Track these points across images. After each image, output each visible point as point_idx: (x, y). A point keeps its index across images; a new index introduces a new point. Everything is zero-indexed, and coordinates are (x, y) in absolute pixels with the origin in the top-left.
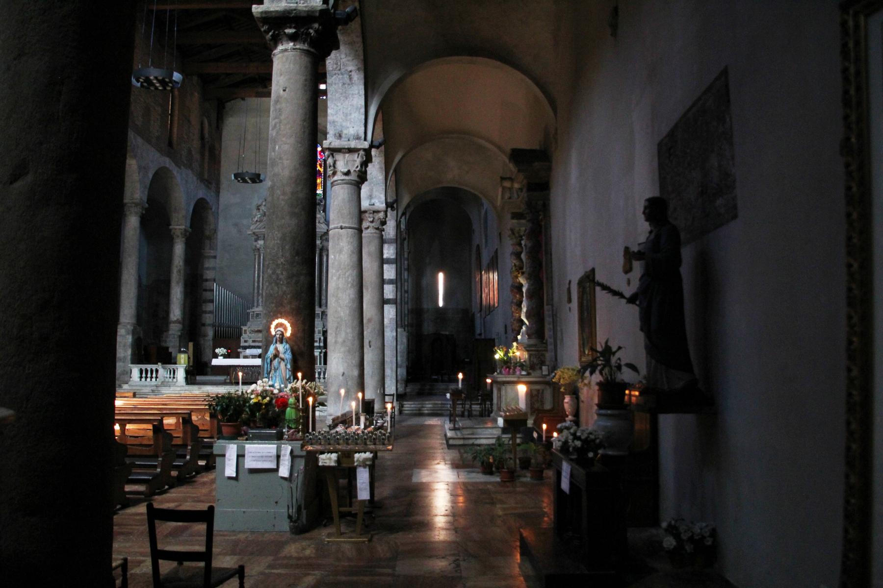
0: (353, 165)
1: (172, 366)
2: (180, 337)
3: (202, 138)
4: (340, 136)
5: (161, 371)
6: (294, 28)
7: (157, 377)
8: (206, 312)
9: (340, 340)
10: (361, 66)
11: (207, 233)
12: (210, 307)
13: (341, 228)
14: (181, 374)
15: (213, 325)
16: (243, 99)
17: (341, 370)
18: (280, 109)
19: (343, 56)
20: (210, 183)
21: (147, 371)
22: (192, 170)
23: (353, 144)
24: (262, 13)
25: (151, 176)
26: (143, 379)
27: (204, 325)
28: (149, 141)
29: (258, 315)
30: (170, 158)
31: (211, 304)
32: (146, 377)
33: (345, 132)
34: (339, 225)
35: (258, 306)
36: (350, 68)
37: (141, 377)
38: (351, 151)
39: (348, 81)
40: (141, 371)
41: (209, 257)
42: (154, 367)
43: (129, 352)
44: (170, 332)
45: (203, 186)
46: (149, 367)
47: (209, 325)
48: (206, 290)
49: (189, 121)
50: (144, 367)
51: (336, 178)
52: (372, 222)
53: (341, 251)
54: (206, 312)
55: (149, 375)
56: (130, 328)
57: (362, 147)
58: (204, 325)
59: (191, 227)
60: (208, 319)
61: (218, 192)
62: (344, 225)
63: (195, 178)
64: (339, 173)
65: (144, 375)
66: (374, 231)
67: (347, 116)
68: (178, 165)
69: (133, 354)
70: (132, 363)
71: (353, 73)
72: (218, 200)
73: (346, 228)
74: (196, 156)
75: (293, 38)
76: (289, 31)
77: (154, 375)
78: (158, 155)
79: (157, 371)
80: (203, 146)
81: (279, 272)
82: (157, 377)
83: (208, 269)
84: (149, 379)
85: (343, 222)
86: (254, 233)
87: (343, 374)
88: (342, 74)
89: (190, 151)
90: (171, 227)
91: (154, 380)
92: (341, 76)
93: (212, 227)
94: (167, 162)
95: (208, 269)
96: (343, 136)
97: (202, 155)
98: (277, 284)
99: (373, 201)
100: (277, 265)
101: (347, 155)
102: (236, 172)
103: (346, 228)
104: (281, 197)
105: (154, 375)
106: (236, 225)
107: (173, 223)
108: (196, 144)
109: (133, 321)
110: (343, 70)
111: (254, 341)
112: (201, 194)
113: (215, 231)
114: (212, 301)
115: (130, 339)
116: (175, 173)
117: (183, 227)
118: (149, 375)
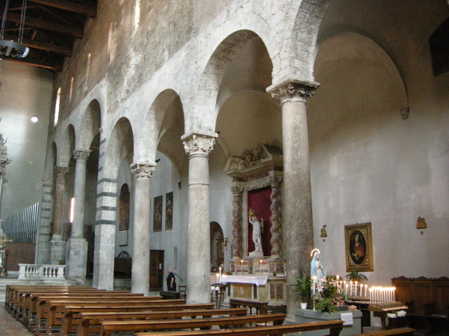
0: (207, 146)
4: (200, 127)
6: (304, 91)
9: (202, 254)
10: (218, 88)
13: (203, 185)
17: (203, 274)
18: (299, 133)
19: (211, 80)
23: (209, 133)
24: (294, 80)
33: (203, 125)
34: (202, 182)
36: (211, 88)
38: (208, 137)
39: (208, 95)
51: (197, 152)
52: (147, 173)
53: (202, 199)
57: (215, 136)
62: (204, 183)
64: (200, 150)
66: (147, 179)
67: (204, 115)
71: (212, 91)
73: (205, 184)
75: (302, 95)
76: (303, 92)
81: (305, 221)
85: (204, 181)
87: (204, 276)
88: (206, 90)
92: (205, 91)
96: (202, 127)
98: (305, 228)
99: (148, 159)
100: (305, 218)
101: (205, 139)
103: (205, 184)
104: (304, 181)
110: (207, 88)
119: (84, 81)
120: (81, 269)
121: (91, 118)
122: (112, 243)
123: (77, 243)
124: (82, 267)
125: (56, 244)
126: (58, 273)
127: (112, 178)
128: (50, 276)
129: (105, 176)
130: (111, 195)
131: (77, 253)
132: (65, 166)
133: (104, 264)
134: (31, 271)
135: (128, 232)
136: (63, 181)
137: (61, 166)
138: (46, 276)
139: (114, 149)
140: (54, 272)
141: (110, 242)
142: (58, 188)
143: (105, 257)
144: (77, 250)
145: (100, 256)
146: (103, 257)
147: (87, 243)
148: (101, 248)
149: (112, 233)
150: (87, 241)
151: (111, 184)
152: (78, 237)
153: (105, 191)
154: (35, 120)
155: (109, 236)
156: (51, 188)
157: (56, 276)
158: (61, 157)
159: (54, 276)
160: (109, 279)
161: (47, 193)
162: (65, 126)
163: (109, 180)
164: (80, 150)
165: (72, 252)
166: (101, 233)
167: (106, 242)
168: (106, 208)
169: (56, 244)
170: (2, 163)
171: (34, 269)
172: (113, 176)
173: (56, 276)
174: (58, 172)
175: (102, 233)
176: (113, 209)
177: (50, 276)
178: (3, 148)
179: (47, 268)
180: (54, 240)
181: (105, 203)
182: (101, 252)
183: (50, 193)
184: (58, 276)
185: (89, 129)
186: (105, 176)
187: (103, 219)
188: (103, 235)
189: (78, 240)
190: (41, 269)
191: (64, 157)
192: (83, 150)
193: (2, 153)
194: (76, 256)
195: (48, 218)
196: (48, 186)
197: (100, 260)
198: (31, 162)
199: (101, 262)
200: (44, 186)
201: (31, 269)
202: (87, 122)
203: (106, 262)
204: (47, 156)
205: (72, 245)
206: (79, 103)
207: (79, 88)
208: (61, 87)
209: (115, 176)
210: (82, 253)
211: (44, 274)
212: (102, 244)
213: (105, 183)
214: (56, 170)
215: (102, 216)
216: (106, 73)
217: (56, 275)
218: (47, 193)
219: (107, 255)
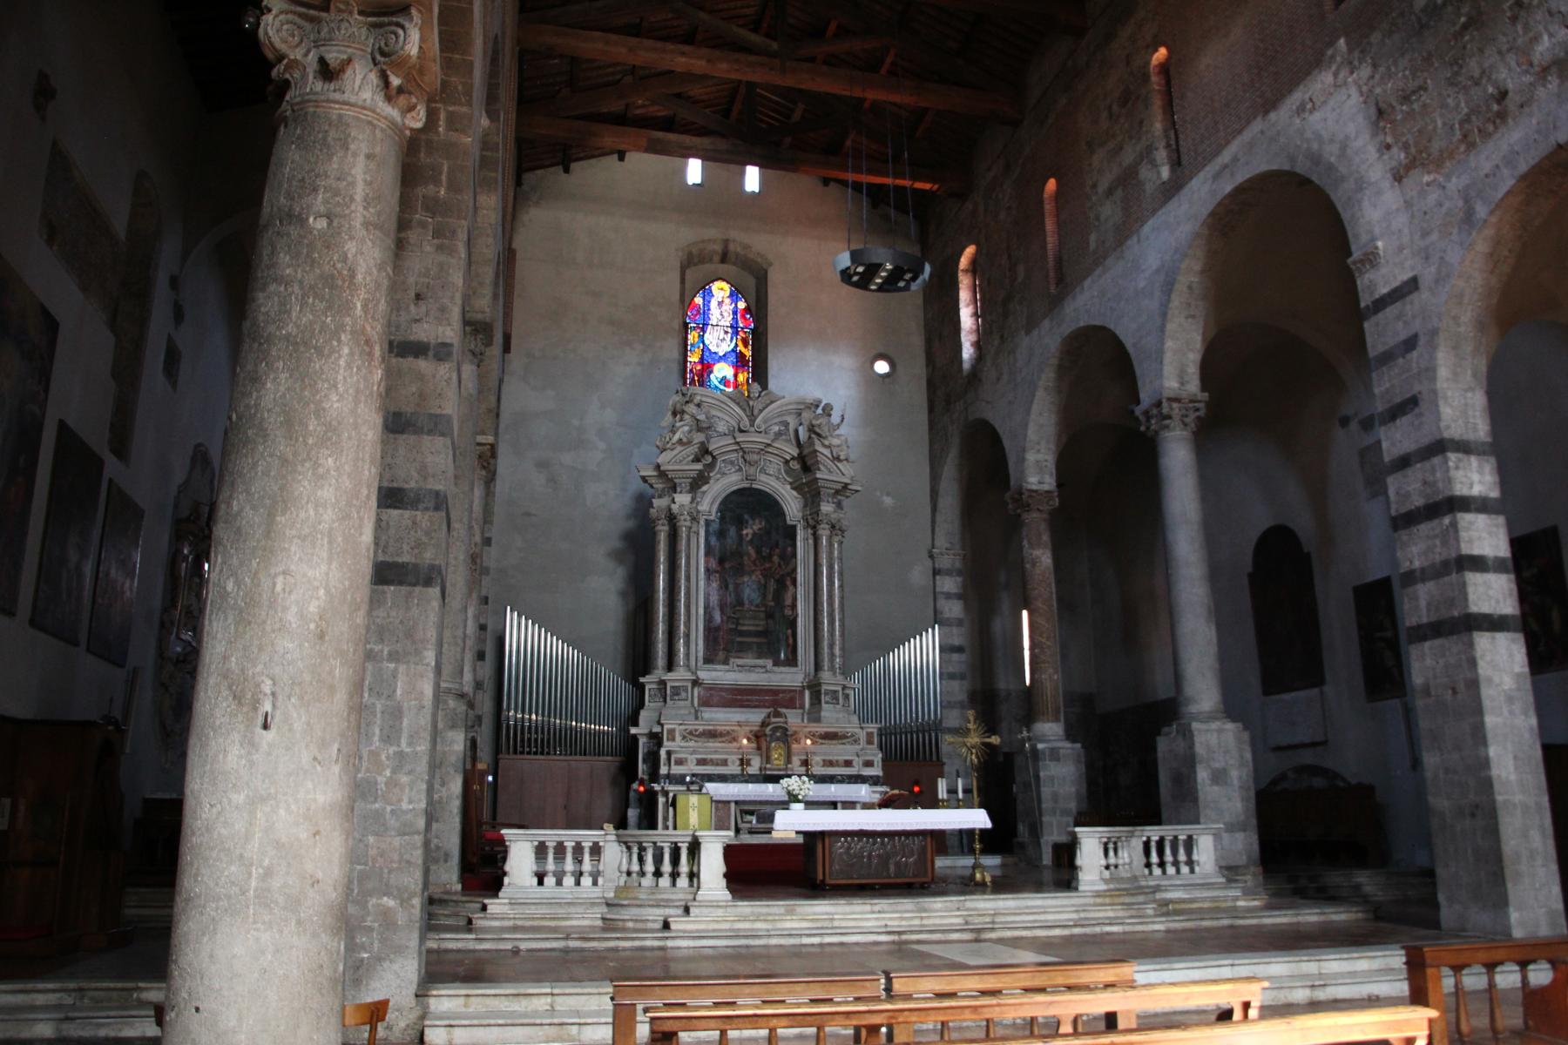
5: (614, 854)
7: (595, 877)
29: (676, 691)
35: (670, 667)
40: (541, 850)
42: (587, 836)
46: (569, 837)
50: (551, 836)
79: (596, 850)
91: (586, 881)
105: (587, 866)
106: (542, 465)
111: (701, 762)
119: (1150, 149)
120: (1240, 836)
121: (1203, 272)
122: (1525, 714)
123: (1213, 739)
124: (1243, 828)
125: (1055, 755)
126: (1195, 857)
127: (1470, 436)
128: (1171, 870)
129: (1448, 427)
130: (1481, 505)
131: (1219, 777)
132: (1046, 487)
133: (1515, 805)
134: (1111, 853)
135: (1322, 693)
136: (1046, 538)
137: (1034, 487)
138: (1157, 871)
139: (1469, 314)
140: (1182, 857)
141: (1517, 707)
142: (1034, 564)
143: (1513, 777)
144: (1217, 765)
145: (1495, 772)
146: (1504, 775)
147: (1246, 736)
148: (1490, 735)
149: (1517, 669)
150: (1246, 728)
151: (1474, 460)
152: (1210, 717)
153: (1460, 490)
154: (882, 367)
155: (1508, 683)
156: (959, 579)
157: (1192, 871)
158: (1031, 457)
159: (1185, 869)
160: (1541, 872)
161: (948, 596)
162: (1044, 343)
163: (1464, 447)
164: (1171, 395)
165: (1202, 775)
166: (1480, 671)
167: (1505, 711)
168: (1478, 564)
169: (1055, 755)
170: (837, 492)
171: (1111, 846)
172: (1475, 429)
173: (1192, 871)
174: (1027, 507)
175: (1483, 669)
176: (1499, 566)
177: (1171, 870)
178: (835, 442)
179: (1155, 838)
180: (1042, 741)
181: (1470, 541)
182: (1492, 751)
183: (959, 597)
184: (1197, 869)
185: (1193, 317)
186: (1448, 427)
187: (1474, 609)
188: (1490, 680)
189: (1215, 725)
190: (1137, 844)
191: (1040, 457)
192: (1184, 395)
193: (838, 459)
194: (1216, 788)
195: (962, 677)
196: (949, 573)
197: (1497, 787)
198: (888, 501)
199: (1499, 798)
200: (936, 572)
201: (1111, 846)
202: (1190, 287)
203: (1518, 798)
204: (935, 478)
205: (1199, 749)
206: (1126, 230)
207: (1110, 192)
208: (978, 245)
209: (1480, 429)
210: (1234, 774)
211: (1148, 865)
212: (1490, 720)
213: (1453, 457)
215: (1472, 597)
216: (1338, 38)
217: (1190, 863)
218: (948, 596)
219: (1516, 768)
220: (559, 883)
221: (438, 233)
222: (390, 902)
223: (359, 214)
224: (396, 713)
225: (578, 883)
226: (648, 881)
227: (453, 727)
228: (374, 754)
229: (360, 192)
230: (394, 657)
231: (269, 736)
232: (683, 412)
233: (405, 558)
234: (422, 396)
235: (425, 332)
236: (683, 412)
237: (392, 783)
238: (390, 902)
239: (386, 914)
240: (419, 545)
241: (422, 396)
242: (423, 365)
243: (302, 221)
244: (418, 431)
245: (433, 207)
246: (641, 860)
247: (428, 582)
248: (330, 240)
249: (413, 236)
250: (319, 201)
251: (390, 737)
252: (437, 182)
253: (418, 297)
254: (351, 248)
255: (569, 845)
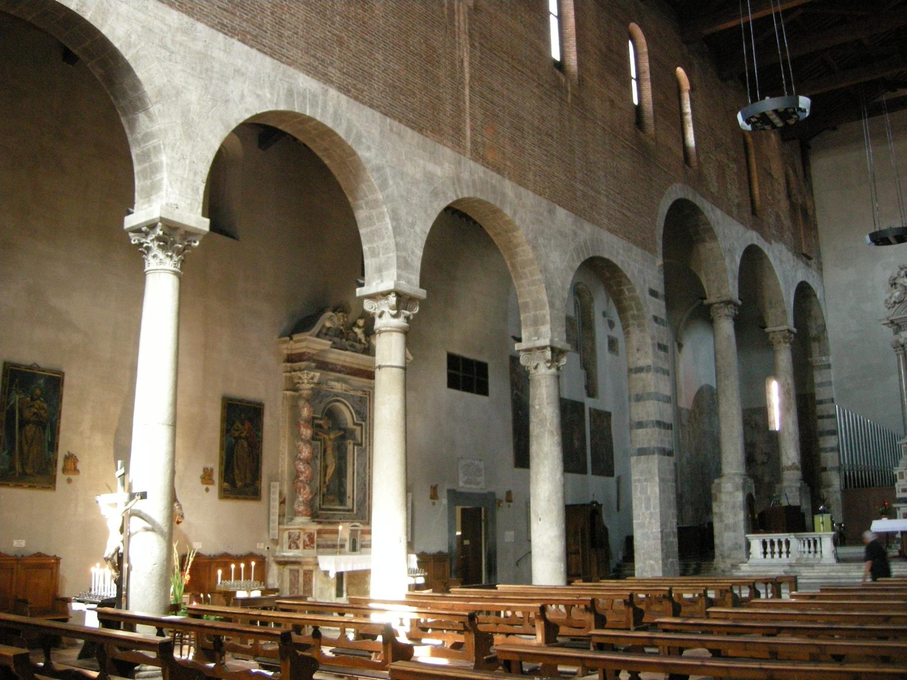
1: (810, 535)
2: (800, 489)
3: (789, 195)
7: (788, 553)
8: (825, 450)
11: (813, 333)
12: (830, 442)
14: (827, 545)
15: (839, 469)
16: (834, 129)
20: (809, 258)
21: (772, 543)
22: (785, 244)
25: (738, 260)
26: (769, 556)
27: (825, 469)
28: (729, 213)
30: (757, 230)
31: (833, 437)
32: (773, 553)
37: (765, 553)
40: (764, 544)
41: (821, 368)
42: (783, 536)
43: (741, 515)
44: (785, 484)
45: (801, 264)
46: (775, 537)
47: (833, 469)
48: (822, 417)
49: (770, 174)
50: (768, 537)
54: (825, 450)
55: (776, 549)
56: (739, 481)
58: (825, 469)
59: (795, 327)
60: (829, 459)
61: (820, 269)
63: (790, 254)
65: (769, 550)
68: (767, 239)
69: (747, 519)
70: (748, 532)
72: (822, 282)
74: (787, 222)
77: (784, 549)
78: (740, 228)
80: (793, 205)
82: (788, 553)
83: (822, 384)
84: (776, 556)
86: (892, 322)
89: (778, 216)
90: (767, 330)
91: (784, 556)
93: (819, 322)
94: (753, 237)
95: (822, 384)
97: (794, 220)
102: (873, 231)
105: (784, 549)
107: (769, 324)
108: (784, 204)
109: (742, 470)
112: (800, 277)
113: (824, 328)
114: (834, 433)
115: (740, 497)
116: (766, 251)
117: (785, 327)
118: (776, 549)
214: (806, 339)
220: (773, 557)
221: (639, 326)
222: (652, 562)
223: (545, 402)
224: (648, 499)
225: (780, 557)
226: (805, 556)
227: (737, 490)
228: (643, 514)
229: (545, 396)
230: (646, 480)
231: (540, 523)
232: (895, 284)
233: (645, 446)
234: (644, 387)
235: (641, 363)
236: (895, 284)
237: (649, 523)
238: (652, 562)
239: (651, 566)
240: (650, 441)
241: (644, 387)
242: (643, 375)
243: (534, 407)
244: (645, 400)
245: (634, 317)
246: (809, 546)
247: (654, 453)
248: (540, 410)
249: (631, 329)
250: (536, 402)
251: (647, 508)
252: (632, 309)
253: (638, 350)
254: (544, 411)
255: (776, 540)
